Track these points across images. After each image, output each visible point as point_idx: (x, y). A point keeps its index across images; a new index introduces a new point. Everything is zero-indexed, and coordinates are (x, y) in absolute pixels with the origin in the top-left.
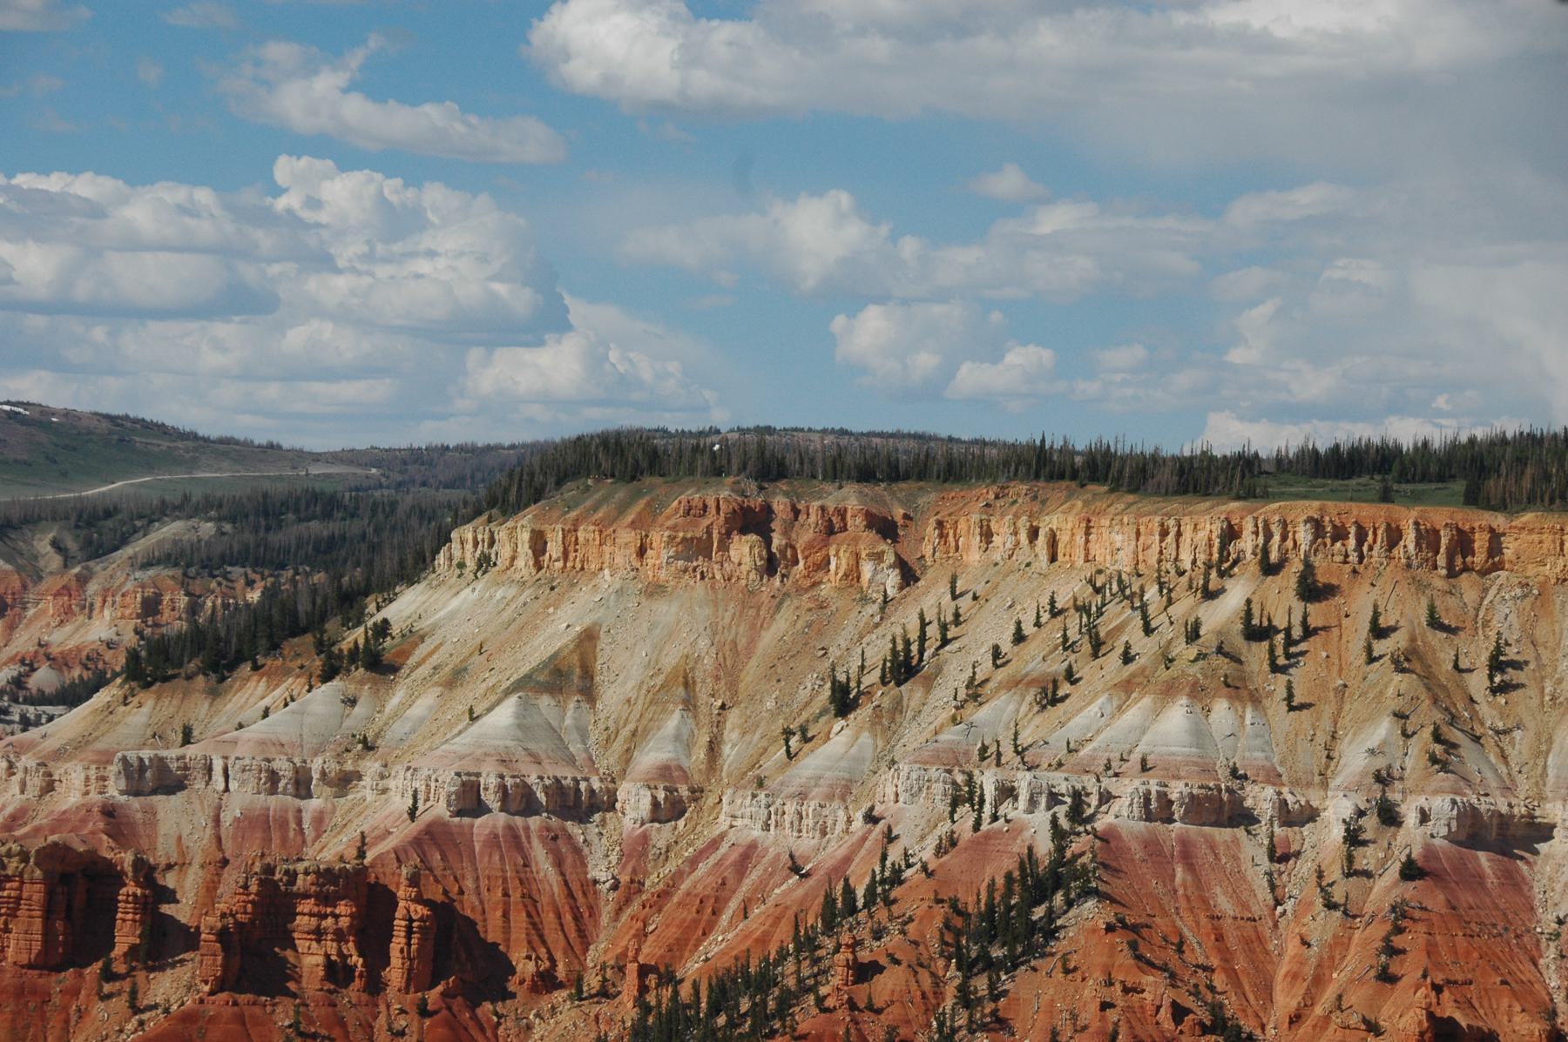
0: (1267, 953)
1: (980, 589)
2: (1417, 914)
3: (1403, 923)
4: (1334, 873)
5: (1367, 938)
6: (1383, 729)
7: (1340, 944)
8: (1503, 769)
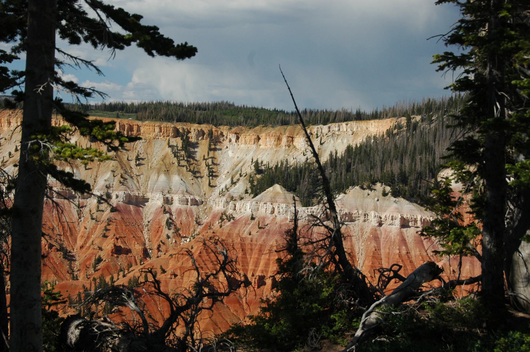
0: (76, 231)
1: (7, 137)
2: (114, 221)
3: (111, 223)
4: (94, 211)
5: (101, 227)
6: (109, 175)
7: (94, 228)
8: (137, 185)
